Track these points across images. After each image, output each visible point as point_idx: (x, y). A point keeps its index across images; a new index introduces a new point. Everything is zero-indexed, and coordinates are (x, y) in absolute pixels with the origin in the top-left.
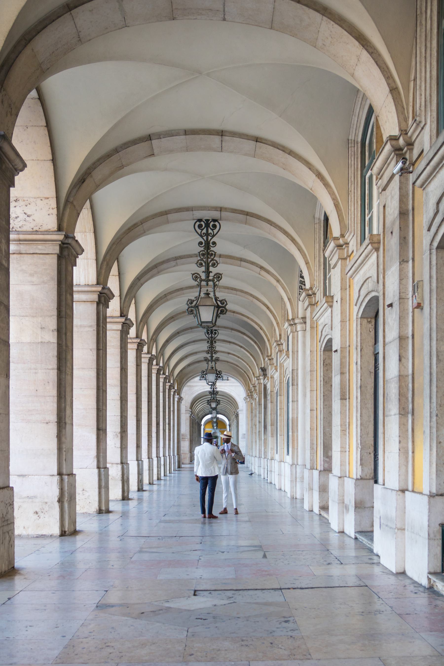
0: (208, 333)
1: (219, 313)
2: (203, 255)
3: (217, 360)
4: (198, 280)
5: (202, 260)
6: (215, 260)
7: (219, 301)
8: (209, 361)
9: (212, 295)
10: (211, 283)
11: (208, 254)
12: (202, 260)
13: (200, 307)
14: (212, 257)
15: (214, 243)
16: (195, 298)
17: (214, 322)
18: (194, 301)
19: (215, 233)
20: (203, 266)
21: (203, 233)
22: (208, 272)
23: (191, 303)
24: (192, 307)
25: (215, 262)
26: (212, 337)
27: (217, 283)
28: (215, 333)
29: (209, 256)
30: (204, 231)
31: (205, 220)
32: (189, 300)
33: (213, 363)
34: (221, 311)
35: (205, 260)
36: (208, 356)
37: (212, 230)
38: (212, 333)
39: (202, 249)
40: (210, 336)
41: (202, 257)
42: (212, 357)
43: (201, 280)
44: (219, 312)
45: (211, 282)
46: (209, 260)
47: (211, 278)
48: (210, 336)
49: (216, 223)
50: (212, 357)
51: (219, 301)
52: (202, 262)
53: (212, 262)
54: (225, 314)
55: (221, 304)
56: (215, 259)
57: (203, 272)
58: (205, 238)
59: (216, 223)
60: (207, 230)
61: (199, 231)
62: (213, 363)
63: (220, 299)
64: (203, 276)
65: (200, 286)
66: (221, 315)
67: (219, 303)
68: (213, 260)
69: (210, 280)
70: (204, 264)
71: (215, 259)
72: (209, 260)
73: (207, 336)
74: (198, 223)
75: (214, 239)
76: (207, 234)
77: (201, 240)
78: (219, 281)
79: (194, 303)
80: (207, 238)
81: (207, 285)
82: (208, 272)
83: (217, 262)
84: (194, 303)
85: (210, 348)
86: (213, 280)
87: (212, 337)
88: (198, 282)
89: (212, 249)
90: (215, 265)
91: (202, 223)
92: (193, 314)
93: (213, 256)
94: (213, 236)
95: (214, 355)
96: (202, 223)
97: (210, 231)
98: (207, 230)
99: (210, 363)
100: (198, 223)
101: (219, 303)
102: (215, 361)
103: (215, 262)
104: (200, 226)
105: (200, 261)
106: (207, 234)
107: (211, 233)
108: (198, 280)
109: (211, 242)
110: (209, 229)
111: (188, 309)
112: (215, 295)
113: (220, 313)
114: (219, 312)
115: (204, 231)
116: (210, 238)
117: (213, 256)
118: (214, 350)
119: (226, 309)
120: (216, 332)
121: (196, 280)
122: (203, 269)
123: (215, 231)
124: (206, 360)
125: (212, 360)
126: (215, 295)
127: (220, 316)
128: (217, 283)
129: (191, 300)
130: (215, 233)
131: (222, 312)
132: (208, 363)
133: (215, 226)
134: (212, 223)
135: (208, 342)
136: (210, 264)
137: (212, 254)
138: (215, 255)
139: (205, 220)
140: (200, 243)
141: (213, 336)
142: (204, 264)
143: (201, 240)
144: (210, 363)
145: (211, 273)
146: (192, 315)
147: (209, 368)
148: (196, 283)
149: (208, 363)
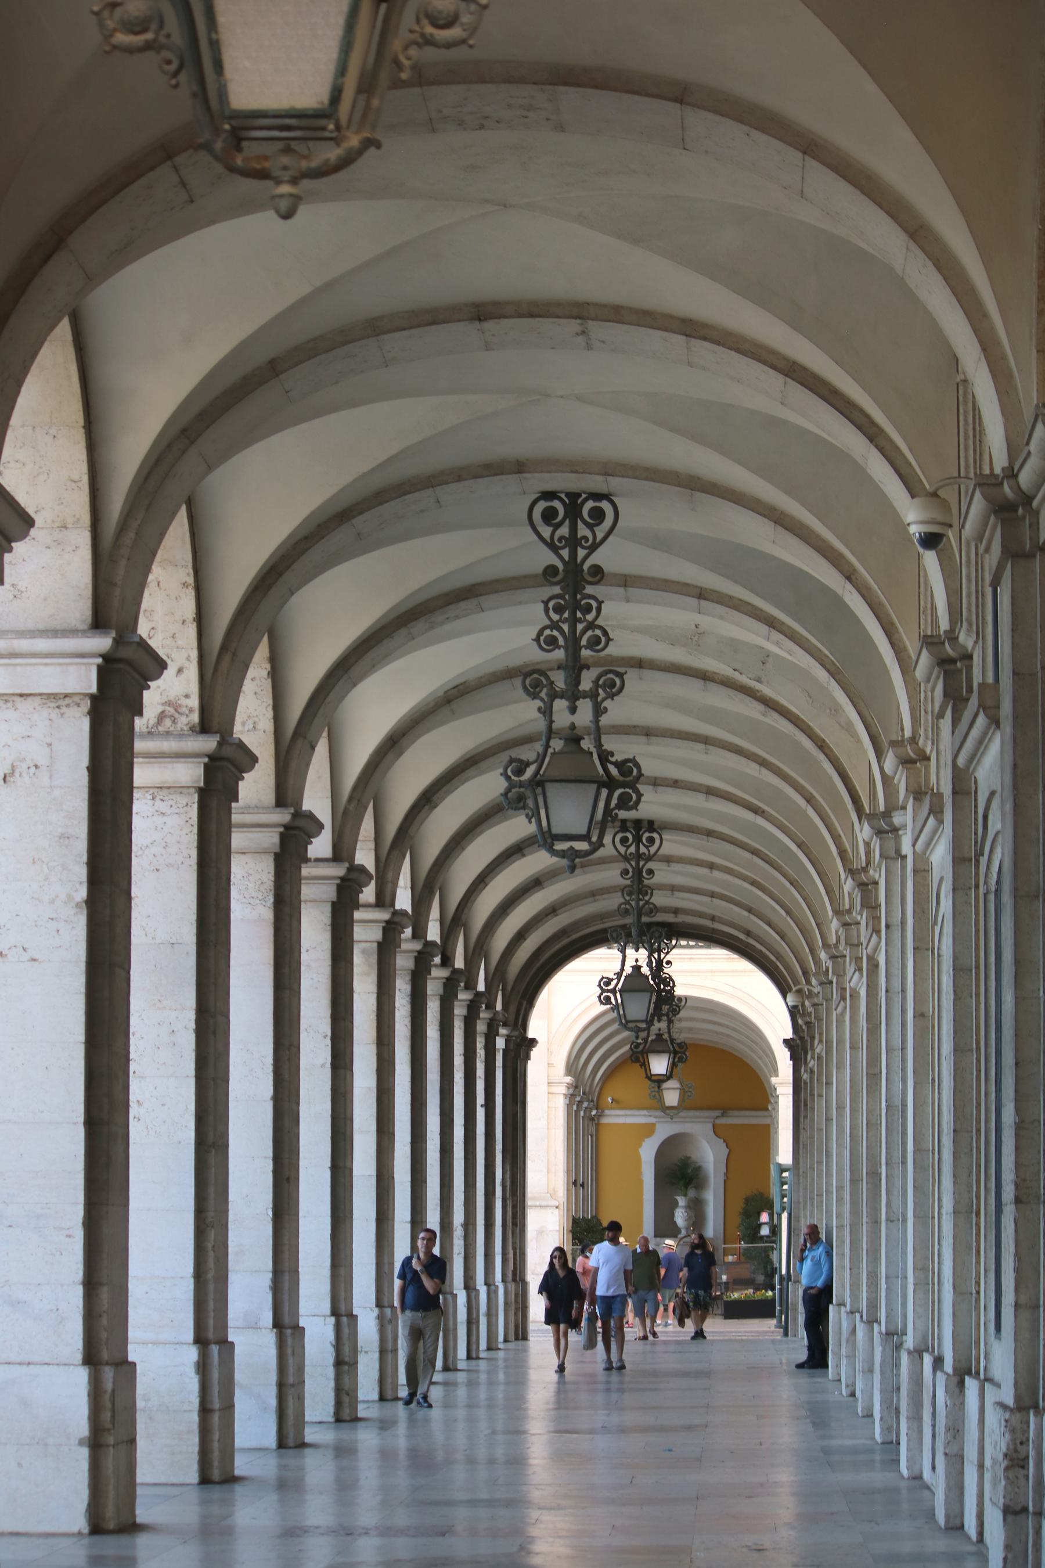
0: (624, 841)
2: (558, 609)
4: (543, 694)
5: (554, 625)
6: (600, 627)
7: (616, 764)
9: (586, 744)
10: (585, 707)
11: (576, 606)
12: (554, 625)
13: (549, 786)
14: (590, 617)
15: (597, 571)
17: (594, 839)
18: (528, 764)
19: (598, 539)
20: (559, 647)
21: (560, 540)
22: (575, 667)
23: (519, 772)
24: (521, 786)
25: (598, 632)
27: (607, 704)
28: (651, 840)
29: (579, 615)
30: (564, 531)
31: (568, 494)
32: (512, 761)
35: (565, 627)
37: (590, 527)
38: (638, 839)
39: (557, 590)
40: (632, 849)
41: (555, 617)
43: (554, 695)
44: (614, 802)
45: (588, 700)
46: (580, 627)
47: (586, 685)
48: (632, 849)
49: (605, 505)
51: (616, 764)
52: (555, 633)
53: (589, 633)
54: (635, 807)
56: (597, 623)
58: (565, 553)
59: (605, 505)
60: (574, 529)
61: (546, 531)
63: (618, 757)
64: (560, 680)
65: (547, 712)
67: (614, 771)
68: (591, 626)
69: (585, 695)
70: (561, 642)
71: (597, 623)
72: (580, 627)
73: (622, 850)
74: (542, 505)
75: (595, 559)
76: (573, 542)
77: (552, 559)
78: (612, 696)
79: (530, 772)
80: (573, 554)
81: (573, 710)
82: (575, 667)
83: (605, 633)
84: (530, 772)
85: (630, 894)
86: (593, 695)
87: (639, 856)
88: (542, 700)
89: (589, 590)
90: (599, 642)
91: (556, 504)
92: (524, 807)
93: (594, 613)
94: (594, 547)
96: (556, 504)
97: (583, 531)
98: (574, 529)
100: (542, 505)
101: (614, 771)
103: (598, 632)
104: (549, 516)
105: (547, 632)
106: (573, 542)
107: (586, 539)
108: (543, 694)
109: (586, 567)
110: (580, 524)
112: (599, 745)
113: (619, 806)
114: (614, 802)
115: (564, 531)
116: (581, 553)
117: (594, 613)
118: (647, 903)
120: (655, 835)
121: (535, 696)
122: (560, 654)
123: (600, 532)
126: (599, 745)
127: (617, 815)
128: (607, 704)
129: (520, 761)
130: (598, 540)
131: (624, 803)
133: (598, 515)
134: (590, 504)
136: (584, 642)
137: (588, 609)
138: (599, 610)
139: (568, 494)
140: (550, 572)
141: (643, 849)
142: (561, 642)
143: (552, 559)
145: (585, 674)
147: (628, 970)
148: (538, 703)
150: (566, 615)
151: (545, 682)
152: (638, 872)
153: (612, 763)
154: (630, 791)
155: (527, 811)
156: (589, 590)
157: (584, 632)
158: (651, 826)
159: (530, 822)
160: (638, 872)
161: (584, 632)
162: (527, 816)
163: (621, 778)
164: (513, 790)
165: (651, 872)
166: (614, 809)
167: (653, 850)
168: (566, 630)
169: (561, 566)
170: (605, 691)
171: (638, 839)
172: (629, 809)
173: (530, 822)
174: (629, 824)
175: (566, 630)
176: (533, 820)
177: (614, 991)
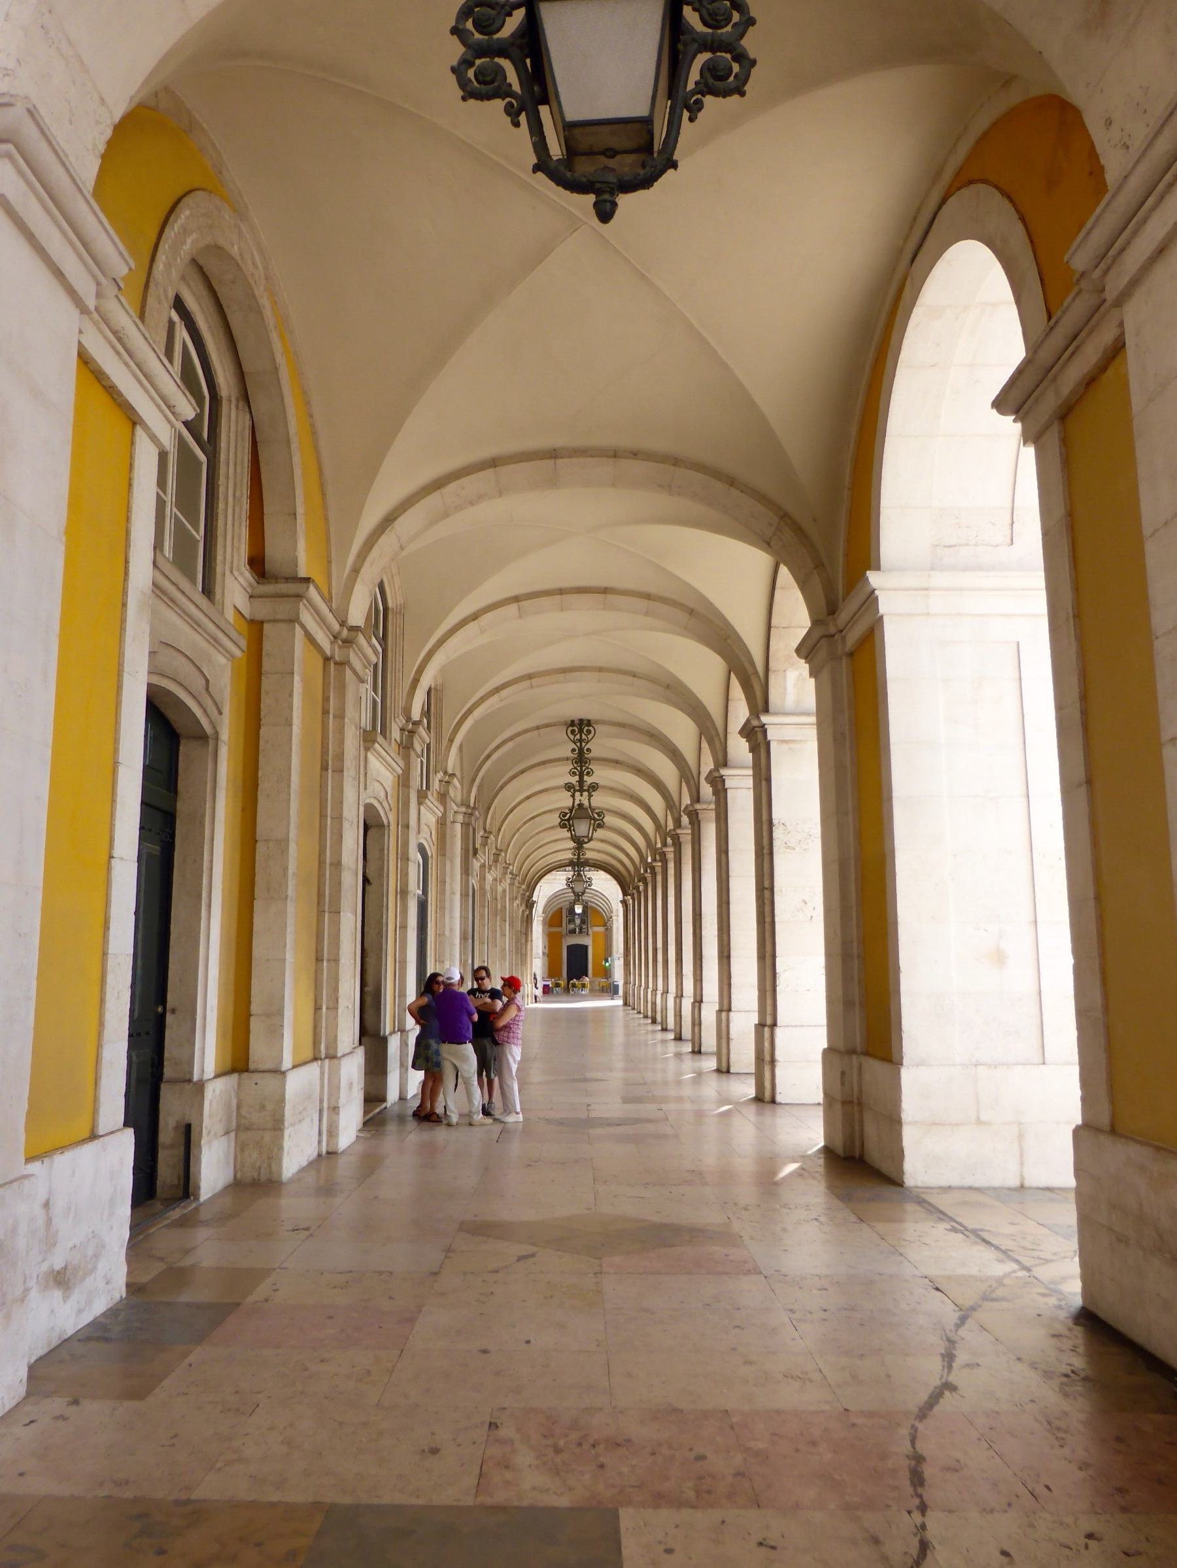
0: (573, 732)
1: (691, 86)
3: (594, 787)
8: (575, 791)
26: (581, 740)
28: (589, 732)
33: (586, 794)
34: (707, 68)
36: (574, 780)
38: (581, 731)
42: (581, 782)
44: (694, 75)
48: (578, 737)
50: (581, 782)
62: (586, 794)
66: (708, 100)
73: (572, 737)
92: (502, 91)
95: (586, 778)
99: (577, 794)
102: (588, 791)
111: (466, 63)
113: (705, 88)
114: (694, 75)
119: (739, 56)
124: (568, 787)
125: (581, 791)
127: (699, 106)
132: (573, 796)
135: (573, 750)
144: (577, 794)
146: (499, 104)
149: (573, 796)
152: (581, 750)
154: (728, 56)
158: (589, 723)
159: (517, 124)
160: (581, 750)
162: (509, 110)
165: (589, 750)
166: (693, 93)
167: (590, 737)
171: (581, 731)
172: (725, 93)
173: (517, 124)
174: (577, 722)
176: (523, 118)
177: (568, 820)
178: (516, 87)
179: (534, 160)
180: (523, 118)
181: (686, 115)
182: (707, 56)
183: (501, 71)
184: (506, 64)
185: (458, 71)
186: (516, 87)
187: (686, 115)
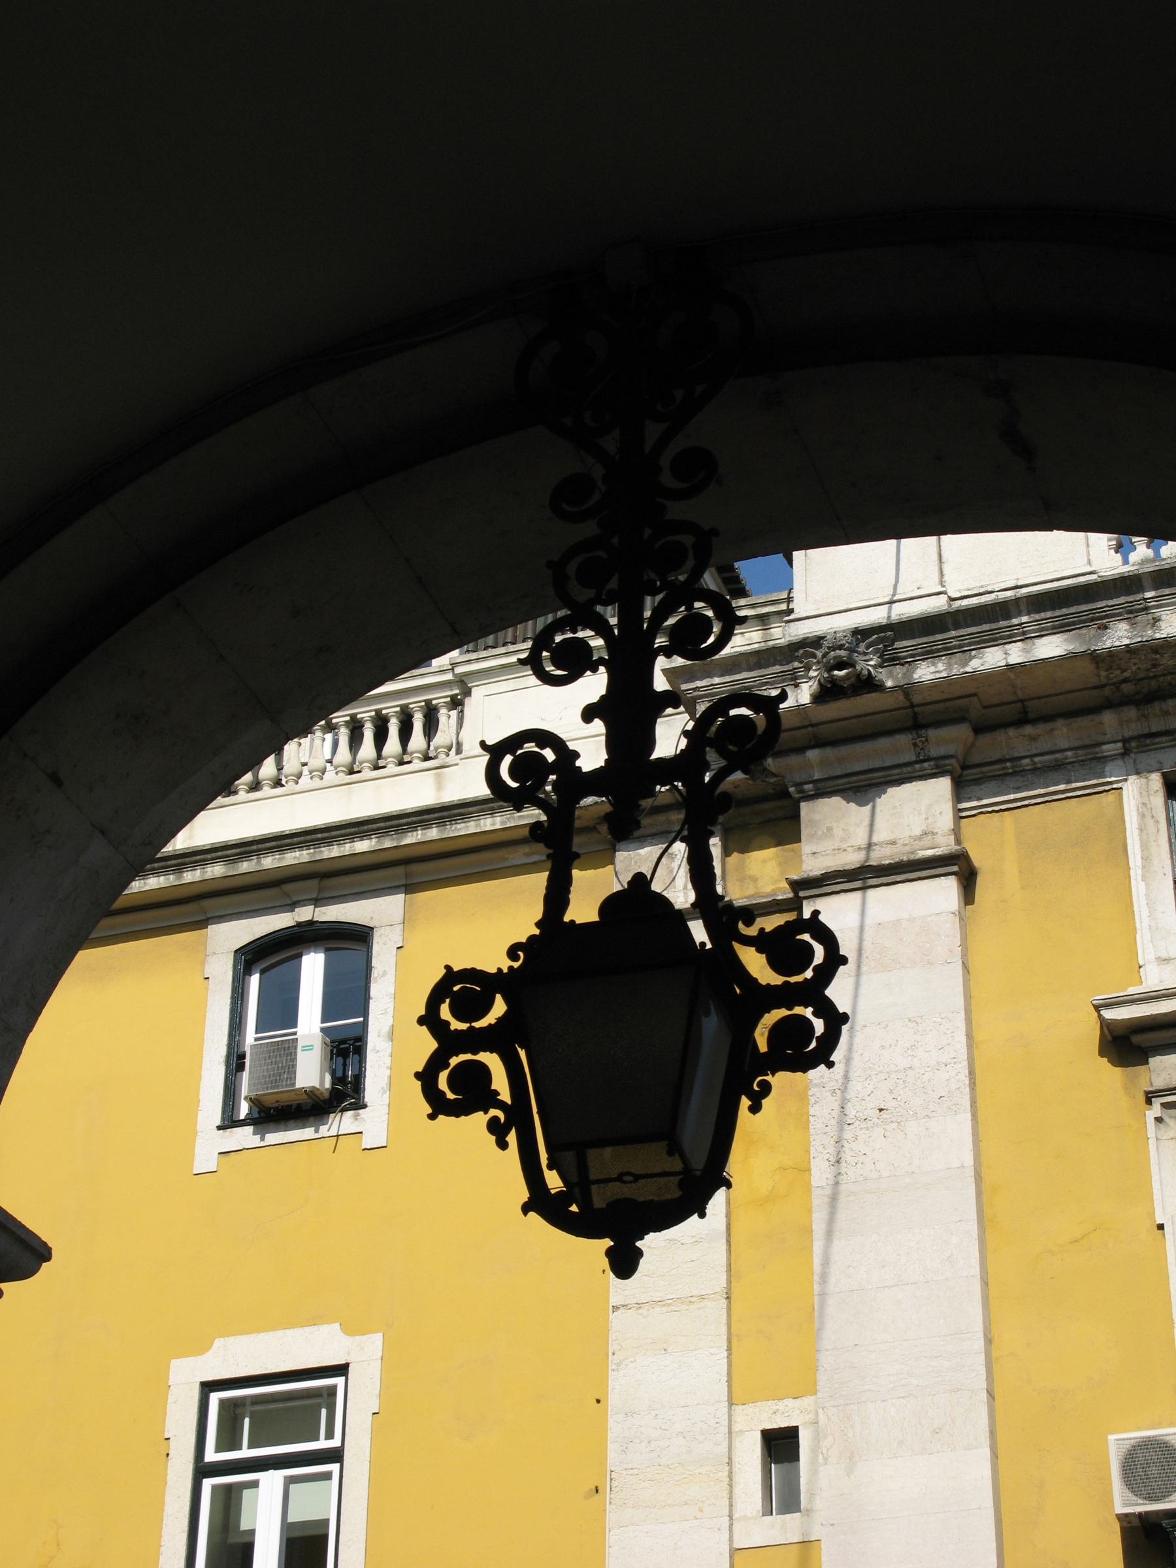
7: (761, 942)
16: (512, 953)
32: (451, 977)
34: (776, 1031)
39: (590, 528)
55: (776, 965)
57: (589, 714)
64: (592, 752)
67: (755, 963)
89: (676, 511)
92: (488, 1099)
101: (755, 963)
109: (665, 461)
116: (653, 431)
119: (827, 1010)
127: (766, 1089)
146: (480, 1119)
150: (613, 584)
151: (549, 755)
153: (747, 941)
154: (808, 1012)
155: (494, 1112)
156: (676, 511)
157: (661, 613)
161: (661, 613)
162: (494, 1127)
163: (777, 980)
164: (454, 1061)
168: (613, 621)
169: (598, 472)
170: (722, 753)
172: (804, 1063)
173: (503, 1145)
175: (613, 621)
176: (512, 1138)
178: (505, 1096)
179: (524, 1195)
180: (512, 1138)
181: (745, 1102)
182: (780, 1013)
183: (484, 1072)
184: (492, 1061)
185: (427, 1077)
186: (505, 1096)
187: (745, 1102)
